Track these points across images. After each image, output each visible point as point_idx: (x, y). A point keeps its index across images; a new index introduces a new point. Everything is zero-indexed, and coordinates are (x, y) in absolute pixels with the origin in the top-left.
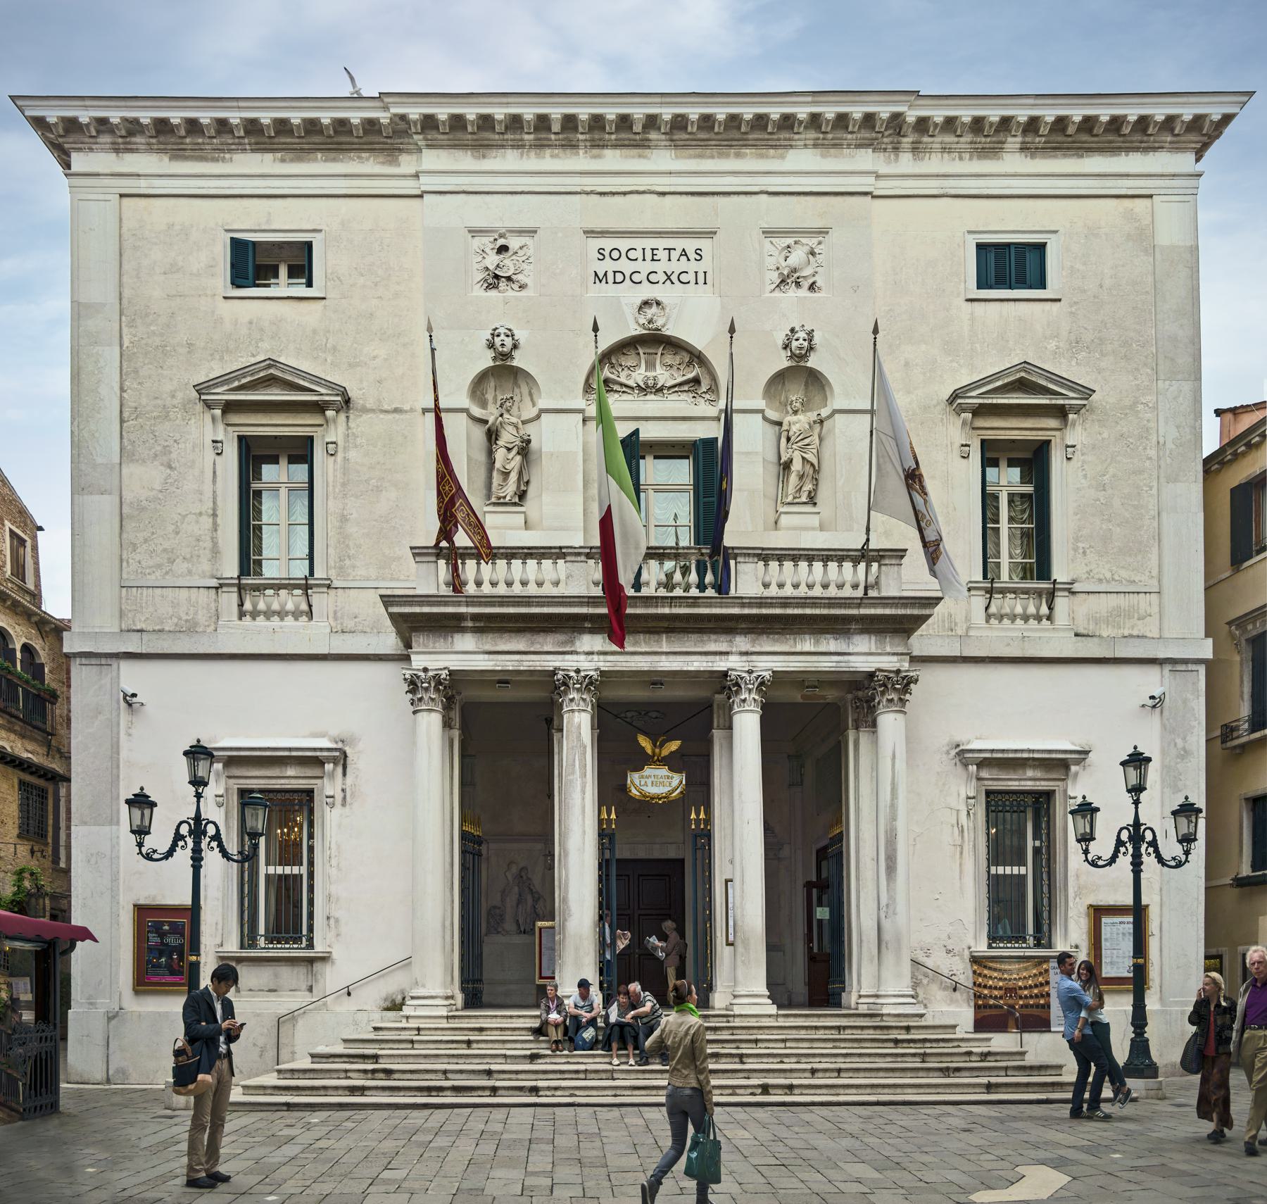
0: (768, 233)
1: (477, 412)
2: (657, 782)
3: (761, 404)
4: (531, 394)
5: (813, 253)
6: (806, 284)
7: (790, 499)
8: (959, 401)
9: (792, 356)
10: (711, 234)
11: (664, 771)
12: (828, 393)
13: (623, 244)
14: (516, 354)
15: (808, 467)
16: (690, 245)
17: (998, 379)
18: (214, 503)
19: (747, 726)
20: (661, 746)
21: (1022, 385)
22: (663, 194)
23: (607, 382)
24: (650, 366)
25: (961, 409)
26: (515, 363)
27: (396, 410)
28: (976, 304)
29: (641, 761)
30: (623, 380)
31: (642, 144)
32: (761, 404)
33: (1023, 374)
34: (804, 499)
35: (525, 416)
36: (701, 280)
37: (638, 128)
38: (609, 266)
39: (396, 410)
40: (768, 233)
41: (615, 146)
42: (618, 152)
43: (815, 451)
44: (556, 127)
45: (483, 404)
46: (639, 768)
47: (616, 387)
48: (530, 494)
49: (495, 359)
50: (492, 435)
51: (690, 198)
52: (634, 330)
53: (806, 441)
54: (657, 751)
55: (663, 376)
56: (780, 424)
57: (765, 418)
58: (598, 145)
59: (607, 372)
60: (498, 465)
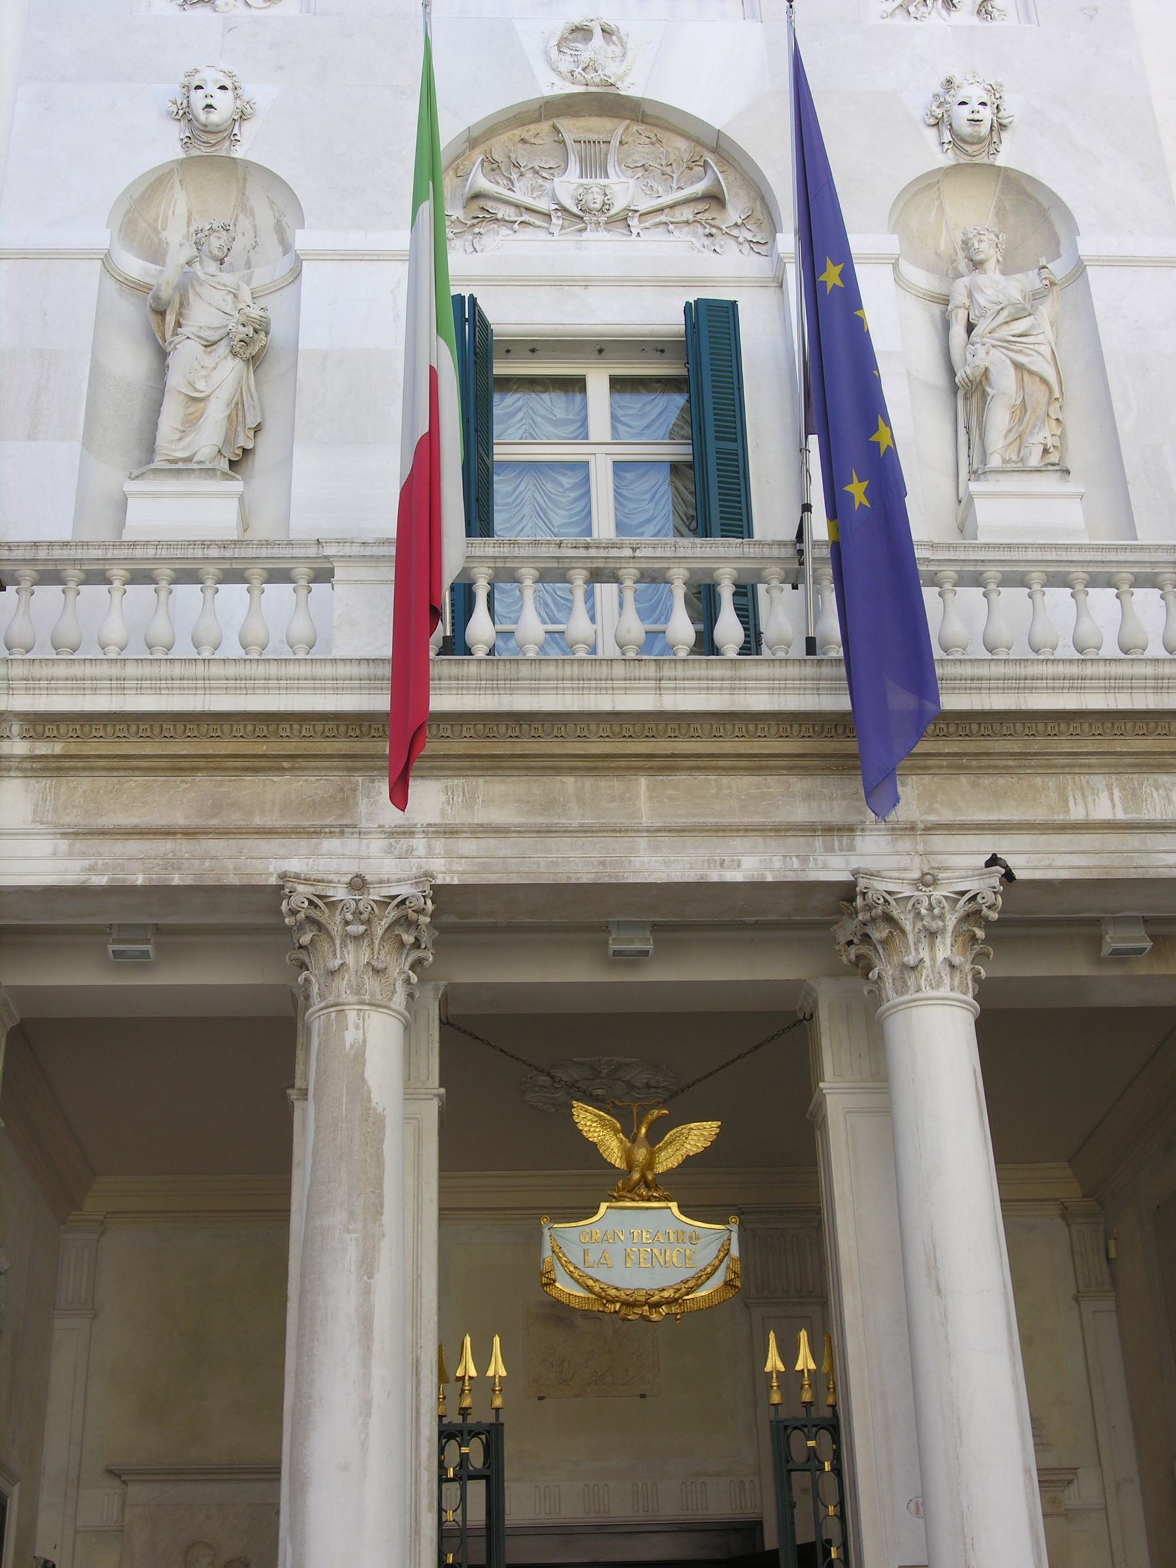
1: (134, 266)
2: (643, 1249)
4: (281, 232)
9: (959, 141)
12: (1059, 228)
14: (247, 131)
19: (938, 1044)
20: (656, 1136)
24: (594, 165)
26: (239, 152)
29: (589, 1184)
30: (519, 196)
34: (1034, 460)
35: (262, 276)
43: (1045, 350)
45: (156, 254)
47: (503, 212)
48: (262, 460)
49: (187, 143)
50: (162, 315)
52: (552, 85)
53: (1020, 326)
54: (641, 1154)
55: (623, 189)
56: (945, 301)
57: (899, 279)
60: (176, 379)
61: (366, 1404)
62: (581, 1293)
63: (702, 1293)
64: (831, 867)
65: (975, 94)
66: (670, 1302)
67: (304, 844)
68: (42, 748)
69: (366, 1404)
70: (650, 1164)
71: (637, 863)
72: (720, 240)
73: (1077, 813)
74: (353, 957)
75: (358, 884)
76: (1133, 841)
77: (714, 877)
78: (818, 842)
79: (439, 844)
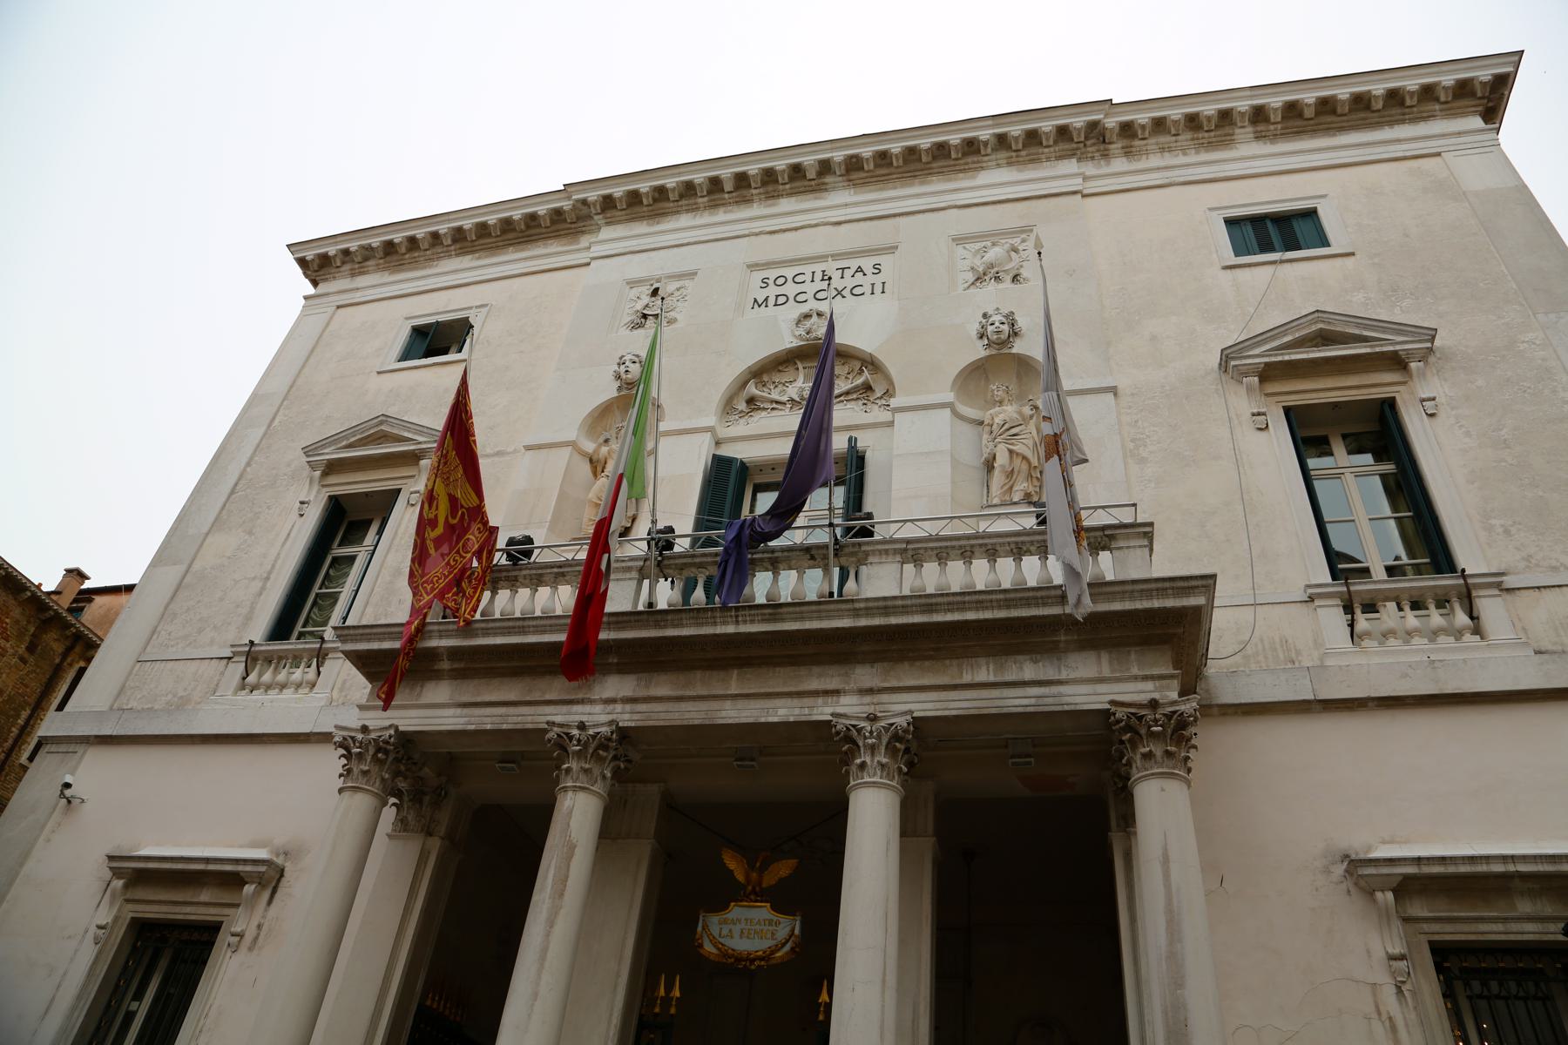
0: (959, 240)
2: (749, 930)
3: (949, 397)
5: (1016, 251)
6: (1008, 278)
7: (996, 501)
8: (1233, 363)
10: (892, 249)
11: (763, 912)
13: (789, 272)
15: (1017, 462)
16: (867, 263)
17: (1285, 334)
18: (273, 566)
21: (1325, 338)
22: (839, 223)
23: (751, 401)
25: (1242, 373)
27: (499, 454)
28: (1238, 271)
29: (724, 895)
30: (775, 396)
31: (818, 188)
32: (949, 397)
33: (1321, 326)
36: (878, 289)
37: (811, 174)
38: (772, 291)
39: (499, 454)
40: (959, 240)
41: (790, 195)
42: (793, 199)
44: (728, 186)
46: (721, 906)
51: (869, 223)
57: (955, 413)
58: (773, 196)
59: (752, 389)
61: (535, 995)
62: (714, 951)
63: (779, 954)
64: (822, 711)
65: (997, 318)
66: (762, 959)
67: (565, 708)
68: (456, 666)
69: (535, 995)
70: (760, 884)
71: (724, 714)
72: (870, 406)
73: (967, 678)
74: (573, 764)
75: (582, 726)
76: (995, 693)
77: (763, 720)
78: (820, 700)
79: (628, 707)
